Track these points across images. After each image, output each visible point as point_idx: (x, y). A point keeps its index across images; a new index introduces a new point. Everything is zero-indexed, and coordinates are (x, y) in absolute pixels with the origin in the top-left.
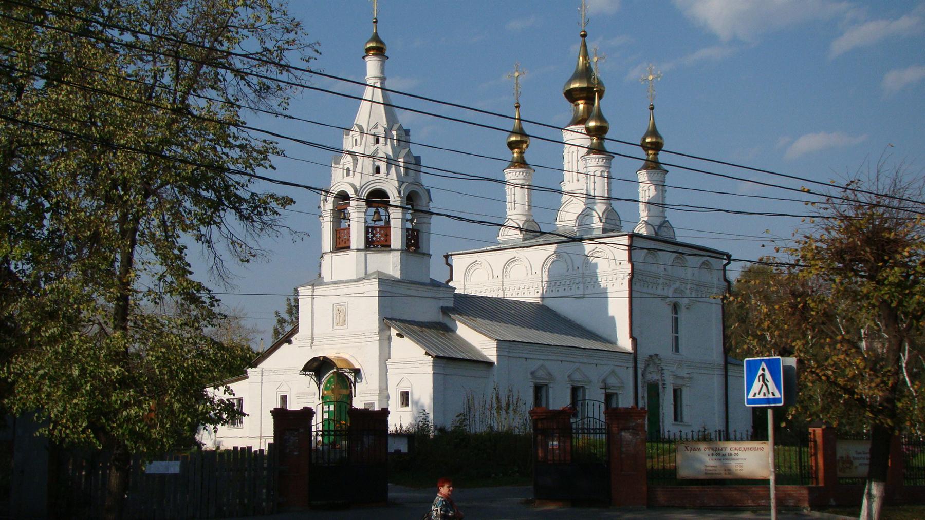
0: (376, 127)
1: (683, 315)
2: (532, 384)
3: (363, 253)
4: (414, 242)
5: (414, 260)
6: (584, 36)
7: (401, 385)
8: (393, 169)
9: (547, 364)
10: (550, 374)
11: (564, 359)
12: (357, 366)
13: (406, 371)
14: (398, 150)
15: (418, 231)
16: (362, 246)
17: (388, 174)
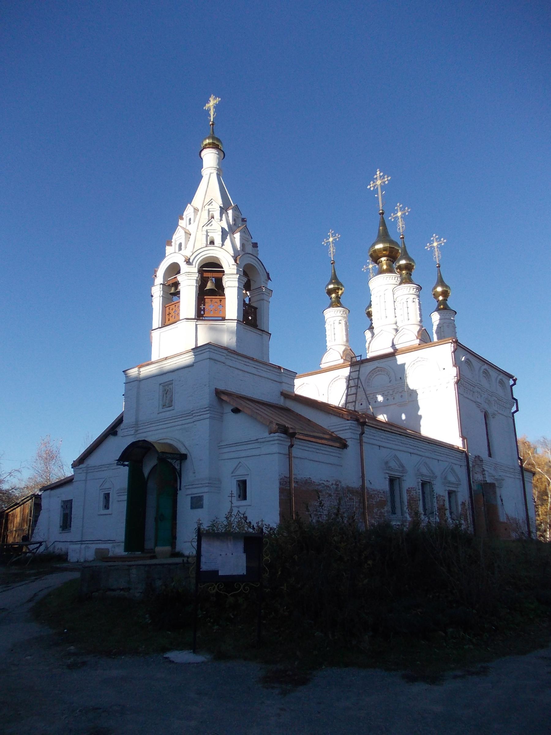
0: (210, 203)
1: (493, 423)
2: (387, 476)
3: (193, 324)
4: (250, 316)
5: (251, 334)
6: (383, 213)
7: (238, 472)
8: (228, 241)
9: (399, 454)
10: (402, 466)
11: (411, 451)
12: (183, 451)
13: (243, 454)
14: (234, 228)
15: (256, 308)
16: (192, 315)
17: (223, 245)
